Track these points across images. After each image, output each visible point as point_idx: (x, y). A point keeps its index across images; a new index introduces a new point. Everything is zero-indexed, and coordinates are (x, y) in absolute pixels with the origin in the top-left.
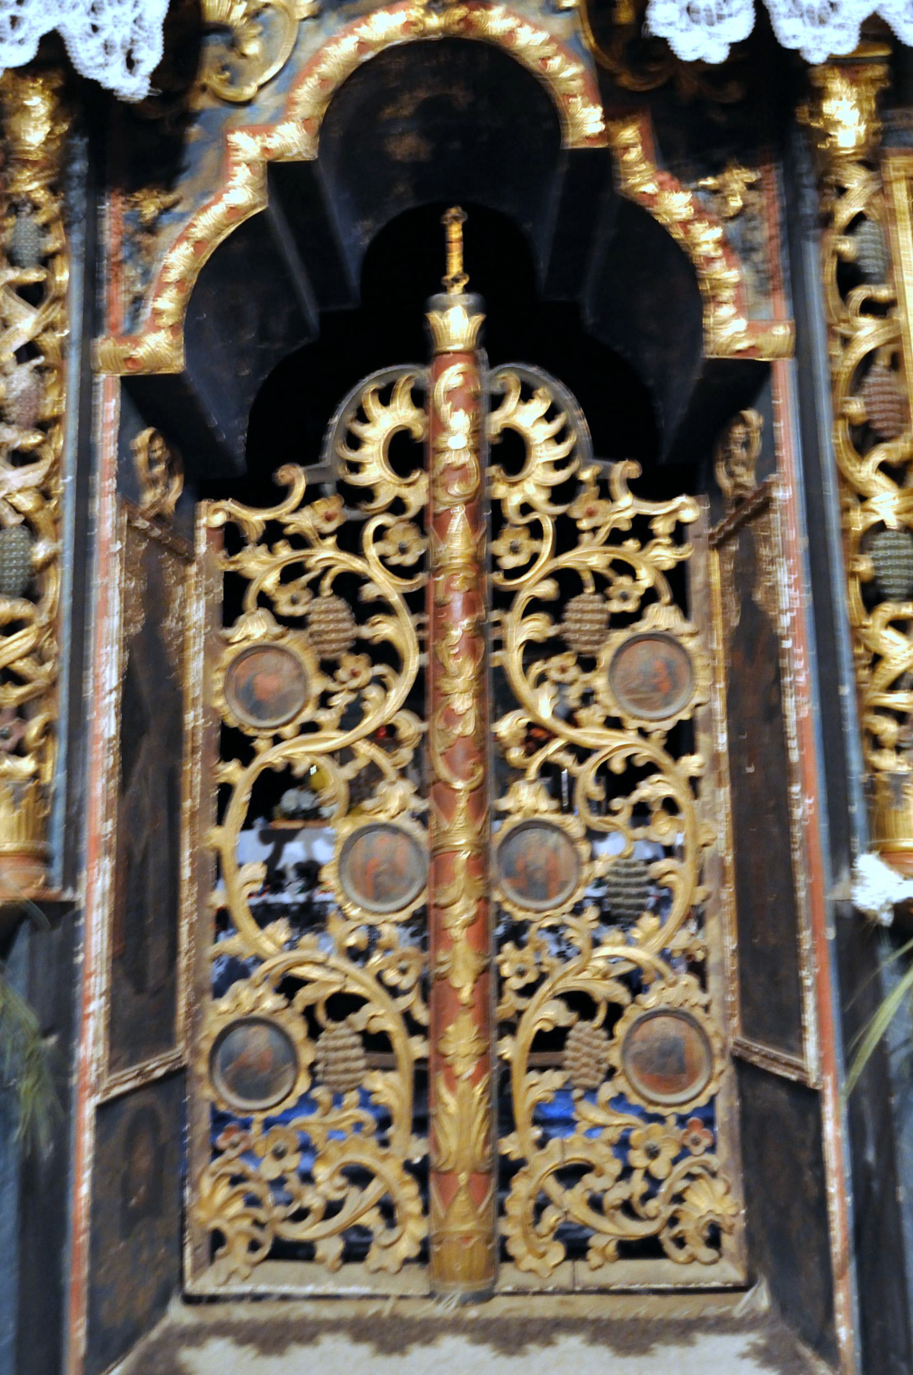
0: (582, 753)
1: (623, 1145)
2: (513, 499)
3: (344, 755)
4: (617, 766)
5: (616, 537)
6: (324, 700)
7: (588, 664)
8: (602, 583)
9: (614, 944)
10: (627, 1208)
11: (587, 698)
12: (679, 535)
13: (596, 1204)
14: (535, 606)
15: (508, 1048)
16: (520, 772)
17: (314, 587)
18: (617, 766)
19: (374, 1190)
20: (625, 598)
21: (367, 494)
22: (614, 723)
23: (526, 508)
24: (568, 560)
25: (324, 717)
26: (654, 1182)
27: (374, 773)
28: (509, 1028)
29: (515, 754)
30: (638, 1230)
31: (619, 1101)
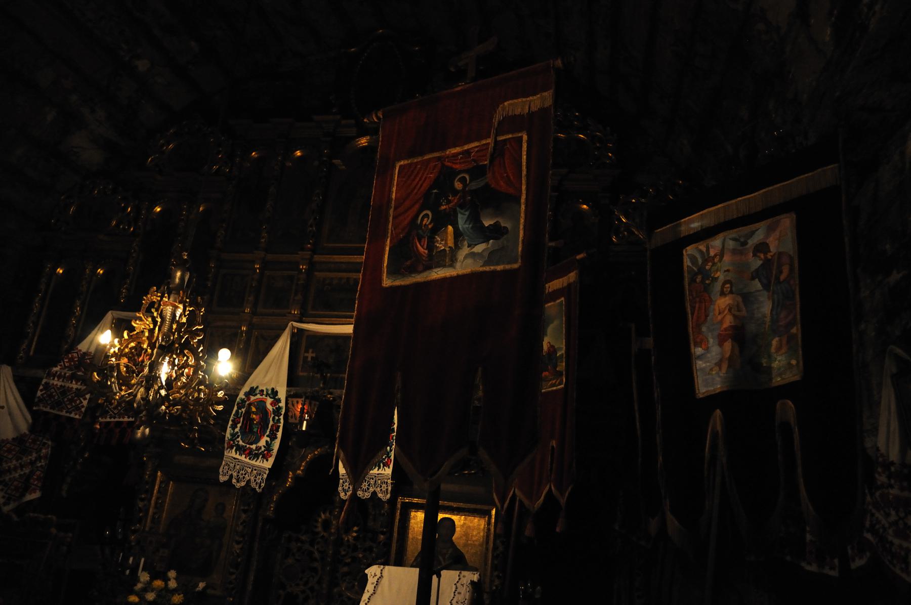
3: (303, 592)
21: (318, 533)
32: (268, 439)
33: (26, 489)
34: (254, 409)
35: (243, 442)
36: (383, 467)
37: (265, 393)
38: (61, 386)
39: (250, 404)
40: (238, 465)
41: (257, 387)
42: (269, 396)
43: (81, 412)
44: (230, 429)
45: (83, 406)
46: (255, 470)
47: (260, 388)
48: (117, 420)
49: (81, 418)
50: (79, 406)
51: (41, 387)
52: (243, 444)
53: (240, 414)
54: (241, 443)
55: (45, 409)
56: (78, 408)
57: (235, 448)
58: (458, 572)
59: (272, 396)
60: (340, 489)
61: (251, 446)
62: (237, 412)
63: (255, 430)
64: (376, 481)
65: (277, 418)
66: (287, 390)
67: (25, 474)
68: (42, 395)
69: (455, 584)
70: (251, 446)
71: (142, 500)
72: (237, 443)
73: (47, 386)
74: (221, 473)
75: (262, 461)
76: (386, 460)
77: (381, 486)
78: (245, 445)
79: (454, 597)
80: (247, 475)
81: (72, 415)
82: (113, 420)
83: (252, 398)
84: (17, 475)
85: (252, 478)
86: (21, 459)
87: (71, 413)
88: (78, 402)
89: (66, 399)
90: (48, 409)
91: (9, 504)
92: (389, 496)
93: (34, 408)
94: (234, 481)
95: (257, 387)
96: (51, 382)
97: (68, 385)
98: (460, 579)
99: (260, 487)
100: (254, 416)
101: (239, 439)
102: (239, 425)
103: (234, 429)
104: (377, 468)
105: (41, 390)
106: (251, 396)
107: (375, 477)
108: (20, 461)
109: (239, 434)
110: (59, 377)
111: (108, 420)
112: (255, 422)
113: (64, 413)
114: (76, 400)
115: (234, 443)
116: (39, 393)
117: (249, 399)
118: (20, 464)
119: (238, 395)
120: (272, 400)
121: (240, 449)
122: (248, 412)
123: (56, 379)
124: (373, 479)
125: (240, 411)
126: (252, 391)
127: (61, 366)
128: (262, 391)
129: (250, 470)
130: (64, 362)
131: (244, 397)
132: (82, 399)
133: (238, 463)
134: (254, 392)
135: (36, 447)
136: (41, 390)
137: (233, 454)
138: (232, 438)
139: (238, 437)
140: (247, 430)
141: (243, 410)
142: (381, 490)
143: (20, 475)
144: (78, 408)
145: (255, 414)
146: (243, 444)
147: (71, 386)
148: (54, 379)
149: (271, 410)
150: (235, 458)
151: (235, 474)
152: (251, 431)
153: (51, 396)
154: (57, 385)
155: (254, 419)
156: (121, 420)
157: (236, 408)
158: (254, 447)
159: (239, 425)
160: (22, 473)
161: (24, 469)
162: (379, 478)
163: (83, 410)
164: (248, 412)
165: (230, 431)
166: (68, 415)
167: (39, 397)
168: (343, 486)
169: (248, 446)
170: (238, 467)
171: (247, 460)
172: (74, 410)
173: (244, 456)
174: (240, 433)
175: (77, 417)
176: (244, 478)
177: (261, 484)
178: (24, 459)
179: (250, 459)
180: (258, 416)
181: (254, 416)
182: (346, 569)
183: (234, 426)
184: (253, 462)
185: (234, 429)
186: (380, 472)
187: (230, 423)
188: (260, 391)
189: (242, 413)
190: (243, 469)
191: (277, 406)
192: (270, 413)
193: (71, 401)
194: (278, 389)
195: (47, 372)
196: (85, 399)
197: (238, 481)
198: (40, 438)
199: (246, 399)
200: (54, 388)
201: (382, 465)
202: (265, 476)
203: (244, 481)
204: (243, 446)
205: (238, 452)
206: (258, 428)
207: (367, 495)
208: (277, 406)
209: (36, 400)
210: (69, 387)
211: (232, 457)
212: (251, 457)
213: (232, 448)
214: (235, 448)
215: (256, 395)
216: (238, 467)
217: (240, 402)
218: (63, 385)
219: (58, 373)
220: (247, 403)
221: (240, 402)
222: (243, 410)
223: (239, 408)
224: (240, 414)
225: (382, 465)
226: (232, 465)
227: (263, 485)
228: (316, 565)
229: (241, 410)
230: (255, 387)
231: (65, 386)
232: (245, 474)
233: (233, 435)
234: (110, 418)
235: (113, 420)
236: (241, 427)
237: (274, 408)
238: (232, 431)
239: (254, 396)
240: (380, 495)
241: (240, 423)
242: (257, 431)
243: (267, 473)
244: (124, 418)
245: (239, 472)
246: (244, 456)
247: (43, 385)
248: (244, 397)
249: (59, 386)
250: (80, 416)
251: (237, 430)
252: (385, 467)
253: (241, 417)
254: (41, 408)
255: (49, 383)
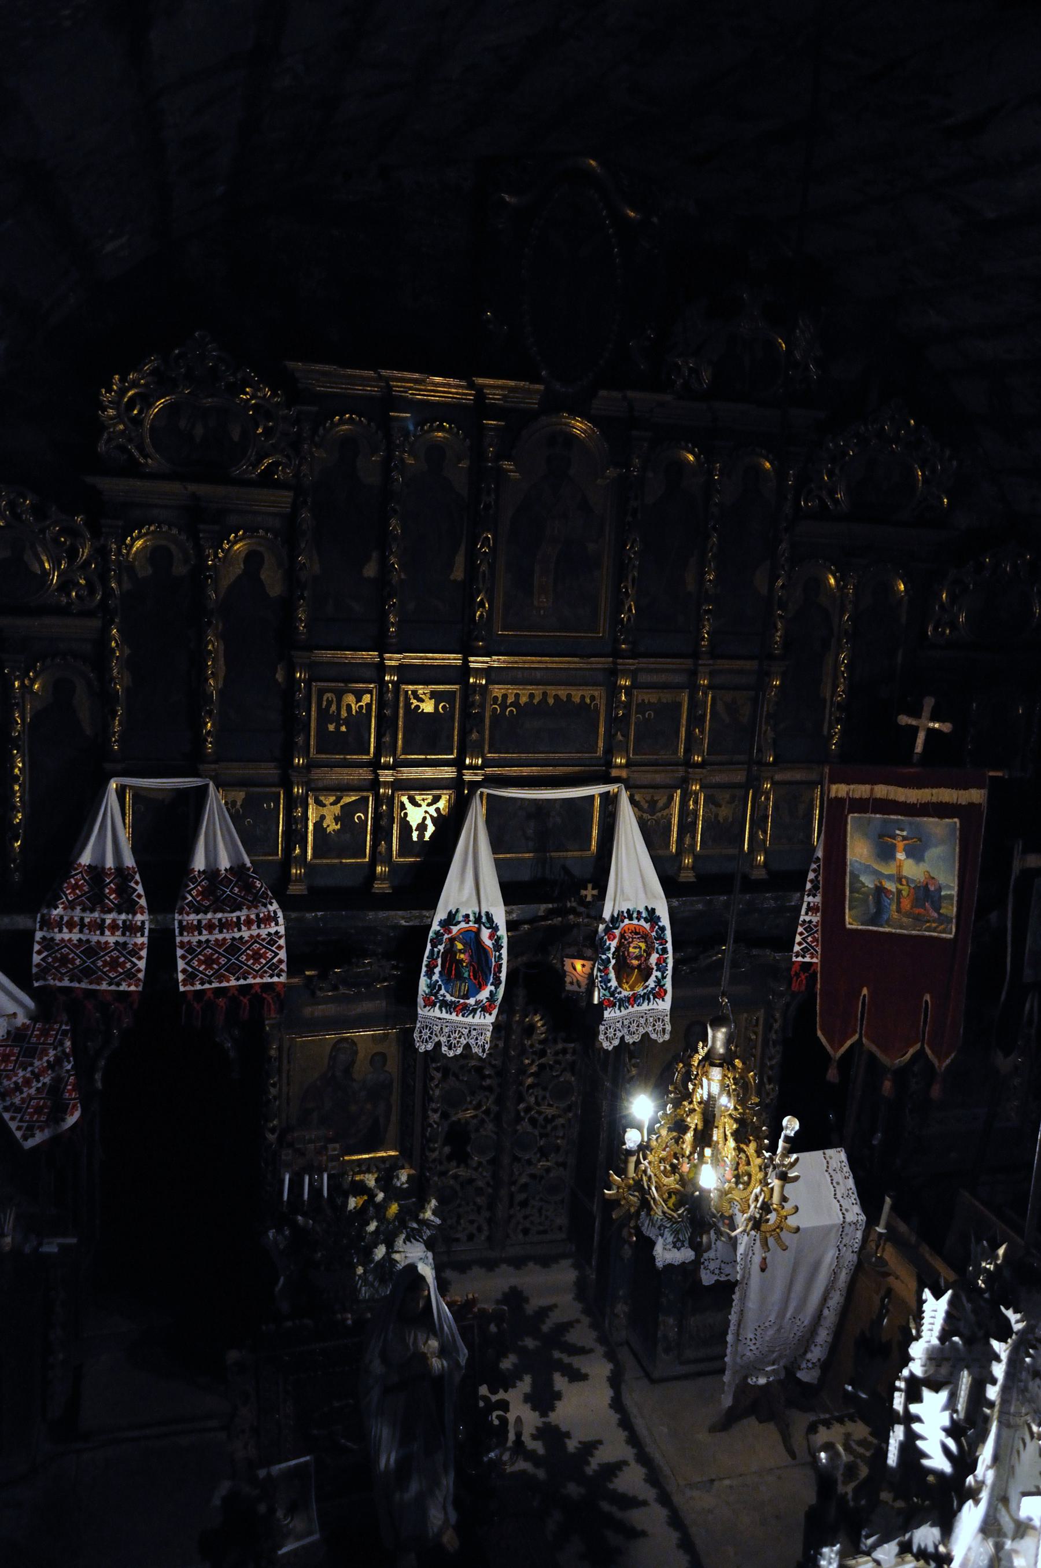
0: (540, 1113)
1: (540, 1210)
2: (528, 1043)
3: (474, 1117)
4: (550, 1117)
5: (556, 1054)
6: (471, 1102)
7: (545, 1089)
8: (551, 1067)
9: (543, 1161)
10: (540, 1224)
11: (544, 1098)
12: (574, 1053)
13: (532, 1223)
14: (532, 1074)
15: (513, 1189)
16: (523, 1119)
17: (469, 1071)
18: (550, 1117)
19: (476, 1225)
20: (557, 1071)
22: (550, 1105)
23: (532, 1046)
24: (543, 1060)
25: (470, 1106)
26: (547, 1217)
27: (483, 1121)
28: (514, 1183)
29: (522, 1114)
30: (541, 1228)
31: (541, 1200)
32: (493, 988)
33: (59, 1110)
34: (460, 946)
35: (452, 996)
36: (654, 999)
37: (472, 918)
38: (80, 940)
39: (452, 940)
40: (447, 1026)
41: (457, 911)
42: (484, 926)
43: (139, 980)
44: (426, 978)
45: (139, 970)
46: (475, 1029)
47: (463, 912)
48: (215, 985)
49: (140, 989)
50: (133, 970)
51: (37, 947)
52: (453, 999)
53: (436, 953)
54: (449, 998)
55: (59, 984)
56: (130, 975)
57: (438, 1004)
58: (821, 1152)
59: (488, 925)
60: (601, 1037)
61: (467, 1001)
62: (432, 951)
63: (466, 975)
64: (647, 1020)
65: (497, 954)
66: (506, 911)
67: (44, 1084)
68: (43, 959)
69: (827, 1171)
70: (467, 1001)
71: (274, 1085)
72: (441, 998)
73: (48, 944)
74: (417, 1039)
75: (482, 1017)
76: (657, 990)
77: (654, 1025)
78: (457, 1000)
79: (835, 1191)
80: (463, 1038)
81: (123, 987)
82: (207, 986)
83: (455, 930)
84: (33, 1091)
85: (472, 1042)
86: (32, 1065)
87: (118, 984)
88: (128, 965)
89: (100, 963)
90: (66, 983)
91: (33, 1136)
92: (667, 1037)
93: (36, 984)
94: (444, 1049)
95: (457, 911)
96: (58, 937)
97: (95, 938)
98: (828, 1162)
99: (484, 1051)
100: (462, 956)
101: (443, 992)
102: (437, 970)
103: (430, 978)
104: (646, 1002)
105: (39, 953)
106: (452, 927)
107: (646, 1014)
108: (29, 1069)
109: (440, 983)
110: (71, 925)
111: (198, 987)
112: (464, 964)
113: (104, 986)
114: (124, 963)
115: (437, 998)
116: (36, 959)
117: (450, 932)
118: (32, 1072)
119: (430, 926)
120: (490, 930)
121: (445, 1005)
122: (450, 952)
123: (65, 930)
124: (642, 1017)
125: (436, 949)
126: (451, 919)
127: (63, 903)
128: (467, 916)
129: (467, 1030)
130: (66, 895)
131: (438, 928)
132: (134, 960)
133: (447, 1024)
134: (454, 918)
135: (50, 1040)
136: (39, 953)
137: (436, 1012)
138: (432, 990)
139: (440, 989)
140: (453, 976)
141: (441, 948)
142: (654, 1030)
143: (38, 1089)
144: (130, 975)
145: (463, 953)
146: (453, 999)
147: (103, 939)
148: (60, 931)
149: (491, 946)
150: (440, 1019)
151: (443, 1039)
152: (459, 977)
153: (64, 960)
154: (70, 940)
155: (462, 961)
156: (225, 984)
157: (429, 947)
158: (472, 1001)
159: (437, 970)
160: (40, 1085)
161: (41, 1078)
162: (651, 1015)
163: (141, 975)
164: (450, 952)
165: (426, 981)
166: (113, 988)
167: (38, 965)
168: (606, 1033)
169: (462, 1001)
170: (446, 1030)
171: (460, 1018)
172: (124, 980)
173: (454, 1014)
174: (442, 981)
175: (133, 988)
176: (458, 1042)
177: (484, 1046)
178: (37, 1063)
179: (463, 1016)
180: (467, 954)
181: (462, 956)
182: (530, 1081)
183: (430, 973)
184: (469, 1019)
185: (430, 978)
186: (651, 1006)
187: (424, 969)
188: (463, 916)
189: (439, 952)
190: (455, 1031)
191: (496, 937)
192: (489, 950)
193: (114, 964)
194: (492, 911)
195: (38, 919)
196: (140, 958)
197: (450, 1048)
198: (56, 1026)
199: (442, 931)
200: (66, 946)
201: (651, 997)
202: (489, 1034)
203: (460, 1047)
204: (451, 1002)
205: (443, 1009)
206: (469, 971)
207: (636, 1038)
208: (496, 937)
209: (34, 970)
210: (98, 942)
211: (435, 1017)
212: (465, 1013)
213: (433, 1005)
214: (438, 1004)
215: (459, 922)
216: (446, 1030)
217: (434, 936)
218: (84, 938)
219: (66, 919)
220: (446, 936)
221: (434, 936)
222: (441, 948)
223: (434, 946)
224: (436, 953)
225: (651, 997)
226: (437, 1029)
227: (487, 1047)
228: (488, 1082)
229: (436, 947)
230: (454, 911)
231: (88, 941)
232: (460, 1037)
233: (432, 986)
234: (202, 984)
235: (207, 986)
236: (440, 972)
237: (494, 941)
238: (429, 981)
239: (455, 925)
240: (654, 1036)
241: (437, 966)
242: (469, 975)
243: (491, 1030)
244: (228, 981)
245: (449, 1036)
246: (454, 1014)
247: (38, 943)
248: (438, 928)
249: (75, 942)
250: (137, 986)
251: (436, 977)
252: (656, 999)
253: (438, 957)
254: (52, 982)
255: (52, 939)
